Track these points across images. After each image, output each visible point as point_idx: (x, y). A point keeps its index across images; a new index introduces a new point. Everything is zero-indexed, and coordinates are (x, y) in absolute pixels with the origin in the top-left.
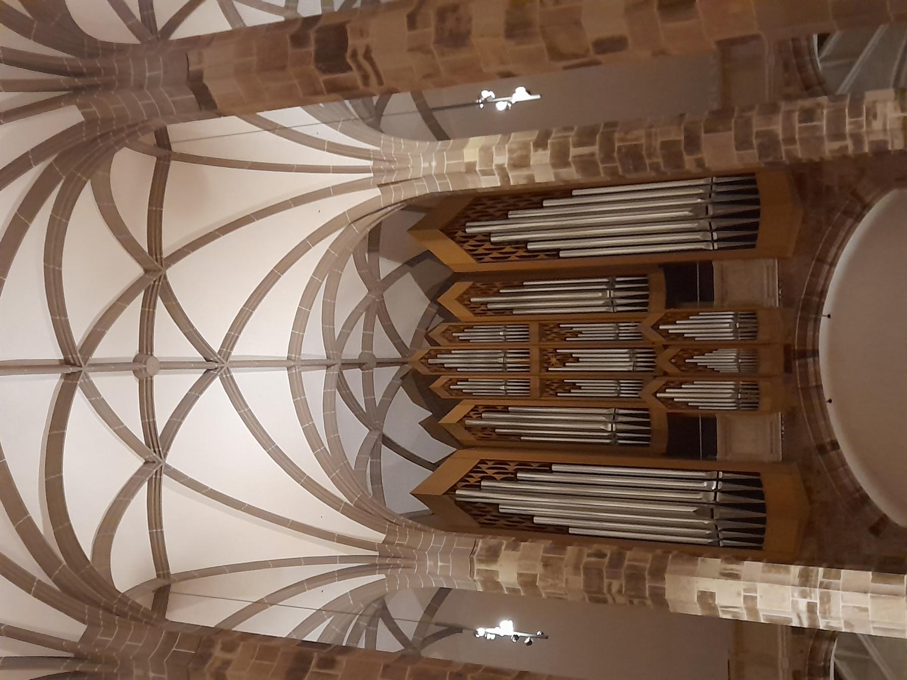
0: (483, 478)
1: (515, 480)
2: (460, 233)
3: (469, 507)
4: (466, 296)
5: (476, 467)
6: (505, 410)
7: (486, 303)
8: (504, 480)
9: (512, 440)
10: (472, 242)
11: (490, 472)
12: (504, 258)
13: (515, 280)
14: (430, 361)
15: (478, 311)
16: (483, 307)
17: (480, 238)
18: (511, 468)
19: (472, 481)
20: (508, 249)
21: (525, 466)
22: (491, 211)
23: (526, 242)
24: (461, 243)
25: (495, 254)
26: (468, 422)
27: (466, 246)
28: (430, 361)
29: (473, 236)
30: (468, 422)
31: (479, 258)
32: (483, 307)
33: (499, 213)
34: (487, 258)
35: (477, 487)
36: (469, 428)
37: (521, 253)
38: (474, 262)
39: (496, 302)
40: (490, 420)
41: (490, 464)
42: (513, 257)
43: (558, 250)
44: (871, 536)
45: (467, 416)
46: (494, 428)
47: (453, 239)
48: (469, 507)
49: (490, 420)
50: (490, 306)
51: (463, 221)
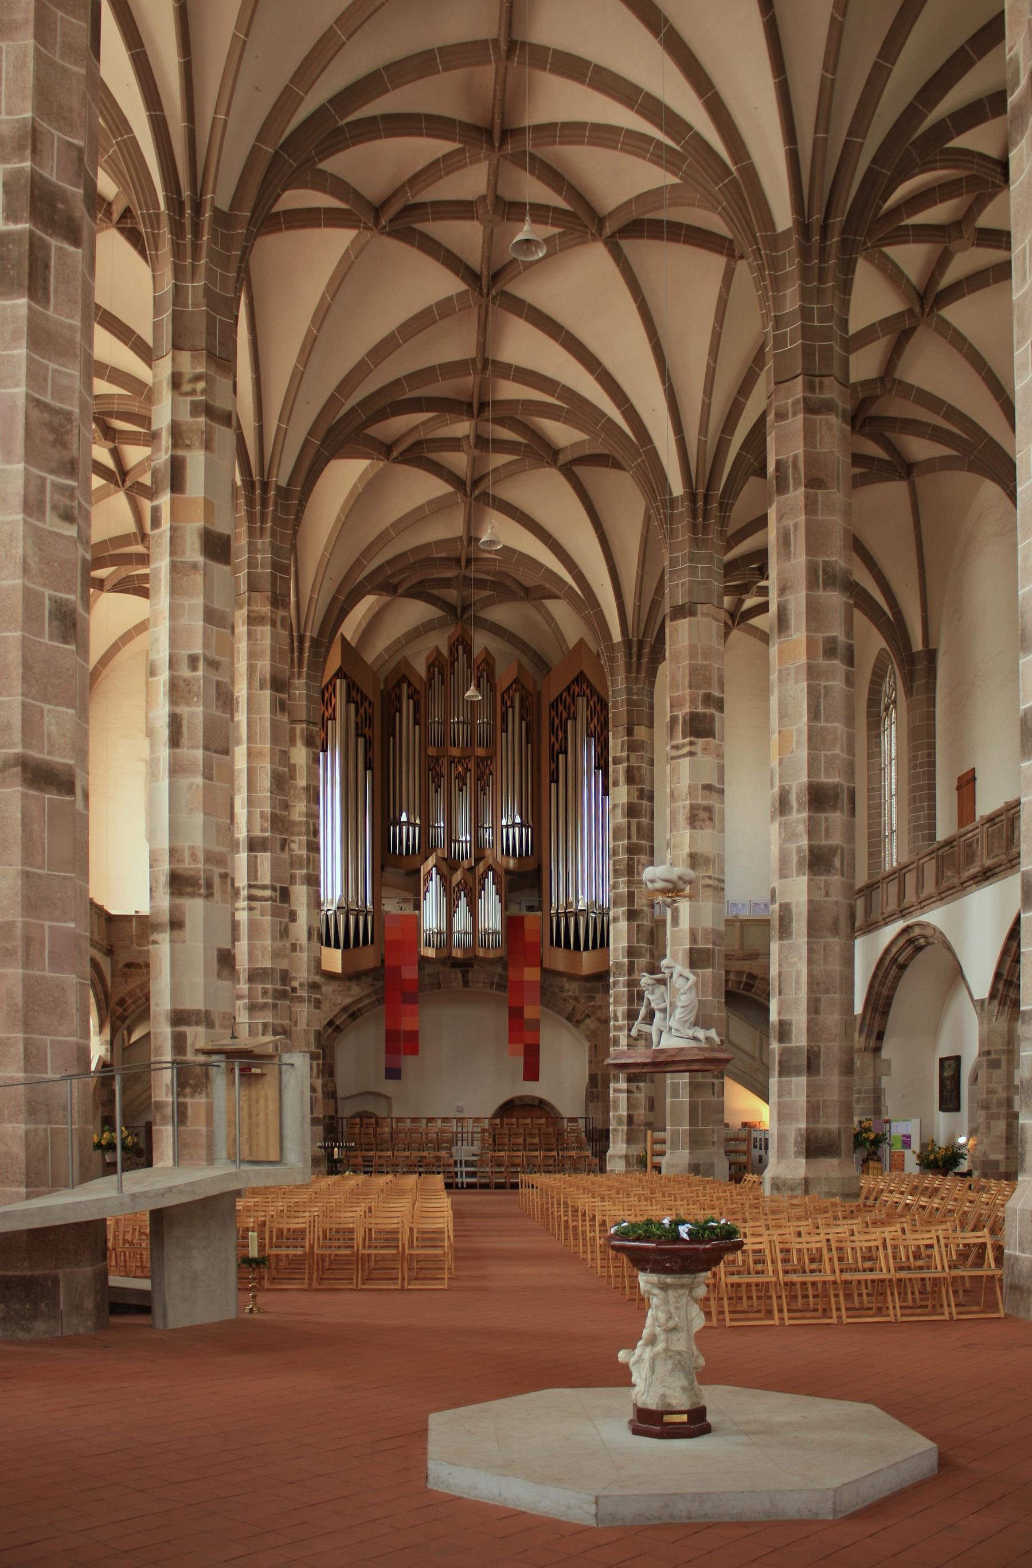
0: (356, 703)
1: (357, 735)
2: (577, 690)
3: (331, 689)
4: (519, 686)
5: (366, 698)
6: (416, 722)
7: (513, 707)
8: (357, 724)
9: (390, 729)
10: (569, 700)
11: (362, 711)
12: (553, 730)
13: (531, 736)
14: (460, 648)
15: (506, 697)
16: (509, 703)
17: (572, 709)
18: (366, 731)
19: (354, 693)
20: (561, 735)
21: (369, 745)
22: (595, 720)
23: (566, 753)
24: (568, 689)
25: (557, 722)
26: (405, 686)
27: (565, 694)
28: (460, 648)
29: (574, 701)
30: (405, 686)
31: (554, 706)
32: (509, 703)
33: (592, 726)
34: (553, 713)
35: (349, 700)
36: (398, 685)
37: (557, 747)
38: (552, 700)
39: (514, 716)
40: (407, 706)
41: (369, 711)
42: (553, 739)
43: (557, 782)
44: (326, 1022)
45: (410, 685)
46: (400, 711)
47: (573, 682)
48: (331, 689)
49: (407, 706)
50: (510, 710)
51: (588, 692)
